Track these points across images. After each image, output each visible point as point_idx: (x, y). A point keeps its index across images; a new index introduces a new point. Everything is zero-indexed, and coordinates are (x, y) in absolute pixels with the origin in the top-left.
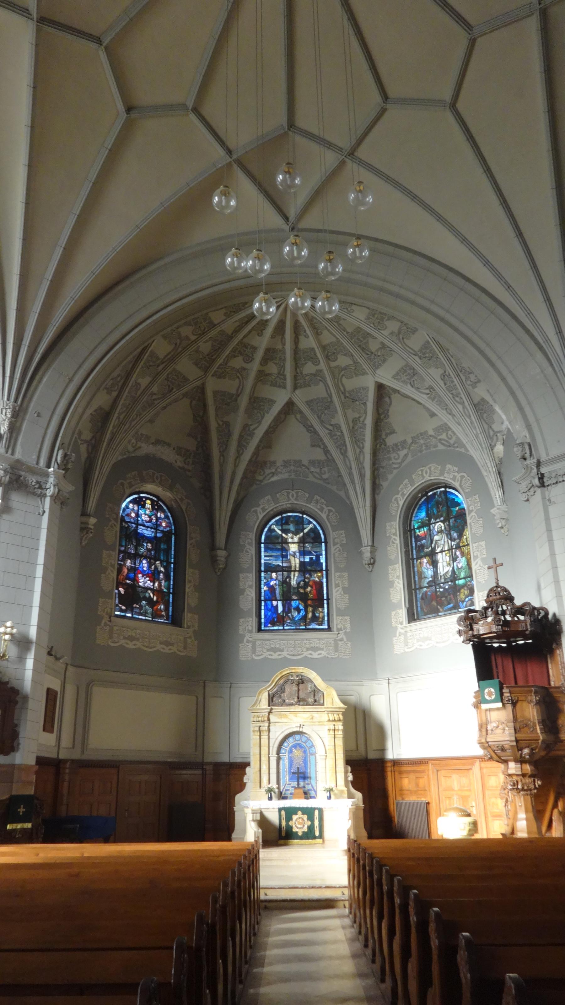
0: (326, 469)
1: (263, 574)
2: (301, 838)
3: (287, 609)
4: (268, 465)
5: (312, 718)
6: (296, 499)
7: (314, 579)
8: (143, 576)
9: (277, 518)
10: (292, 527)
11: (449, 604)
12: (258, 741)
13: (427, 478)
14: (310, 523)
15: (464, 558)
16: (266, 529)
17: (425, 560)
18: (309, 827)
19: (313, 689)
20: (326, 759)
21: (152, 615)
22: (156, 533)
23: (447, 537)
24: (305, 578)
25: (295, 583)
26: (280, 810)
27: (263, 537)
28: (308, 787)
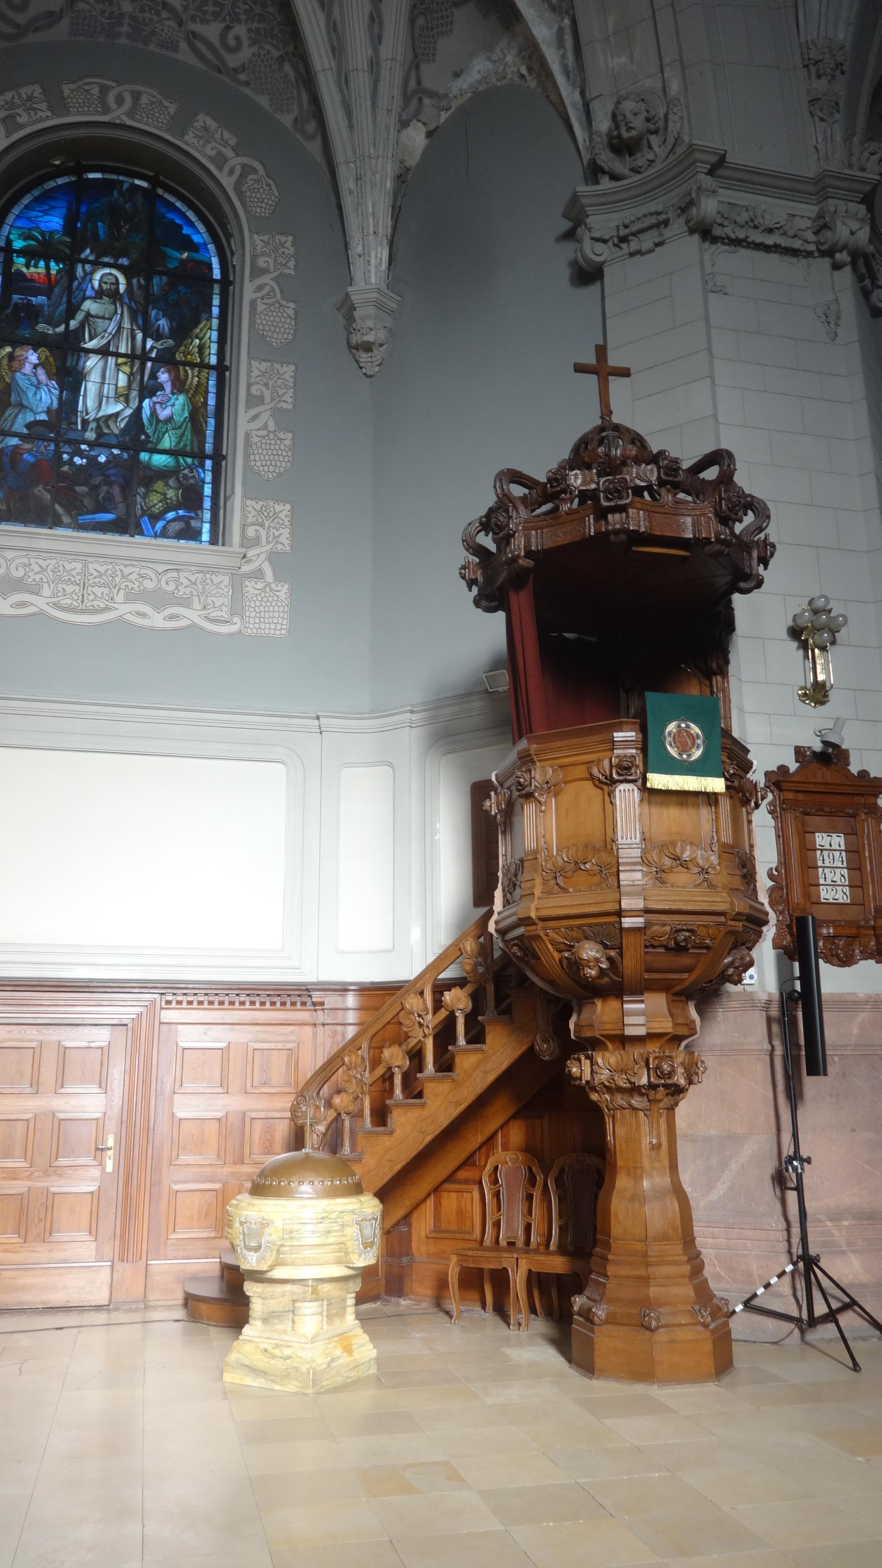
11: (100, 508)
13: (119, 114)
15: (182, 398)
17: (33, 358)
23: (133, 319)
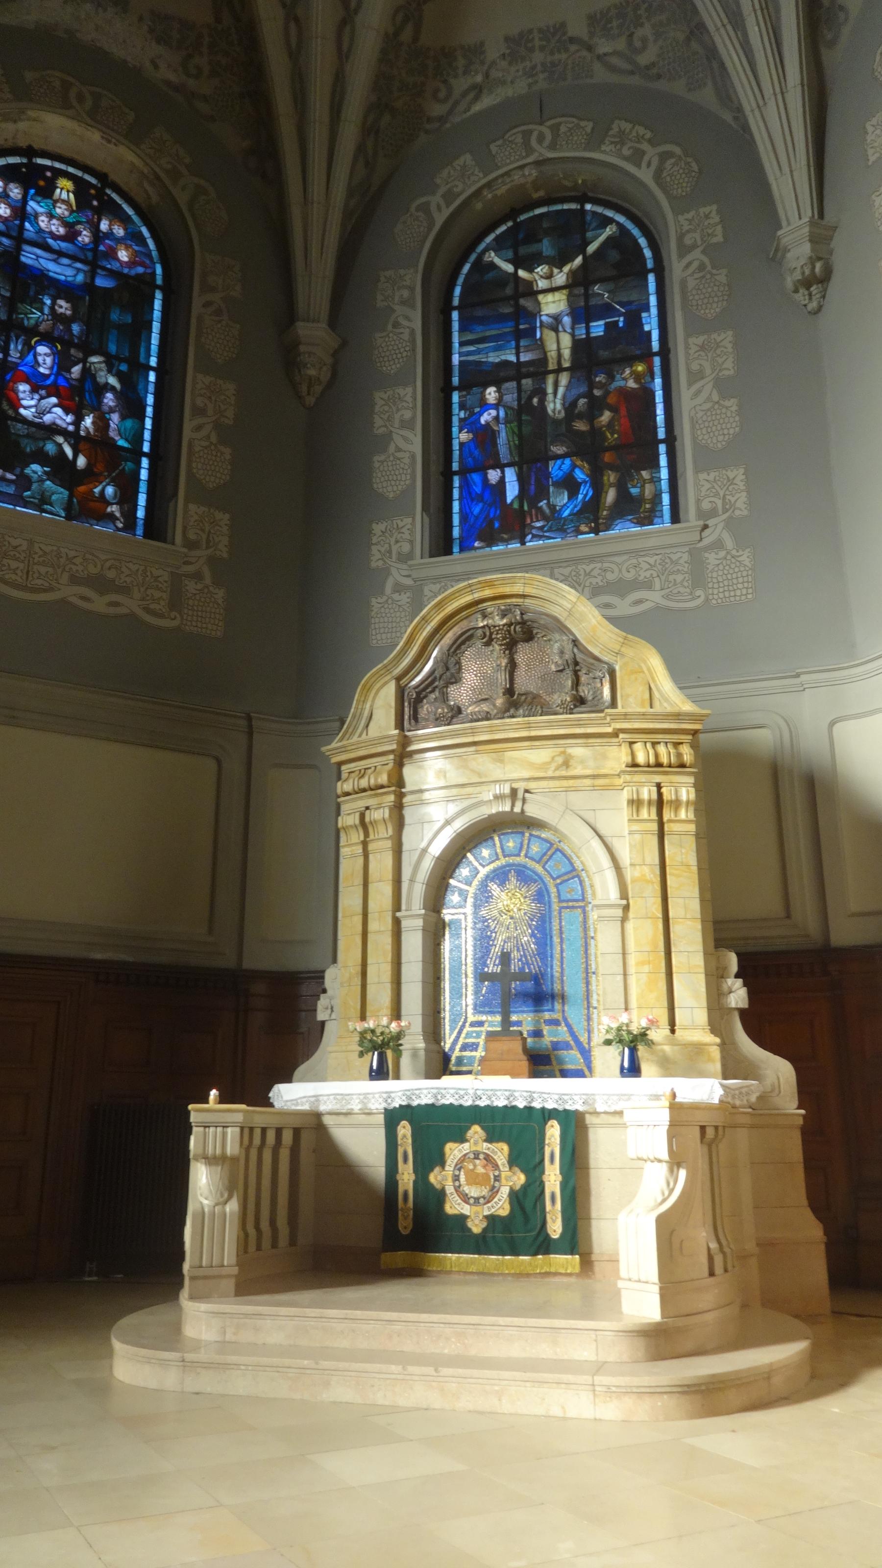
0: (646, 31)
1: (455, 397)
2: (480, 1245)
3: (534, 487)
4: (461, 62)
5: (566, 764)
6: (553, 147)
7: (622, 383)
8: (34, 390)
9: (503, 228)
10: (546, 247)
12: (361, 860)
14: (607, 221)
16: (466, 268)
18: (516, 1197)
19: (568, 656)
20: (624, 920)
21: (68, 507)
22: (93, 274)
24: (592, 385)
25: (559, 406)
26: (392, 1118)
27: (458, 291)
28: (549, 1036)
